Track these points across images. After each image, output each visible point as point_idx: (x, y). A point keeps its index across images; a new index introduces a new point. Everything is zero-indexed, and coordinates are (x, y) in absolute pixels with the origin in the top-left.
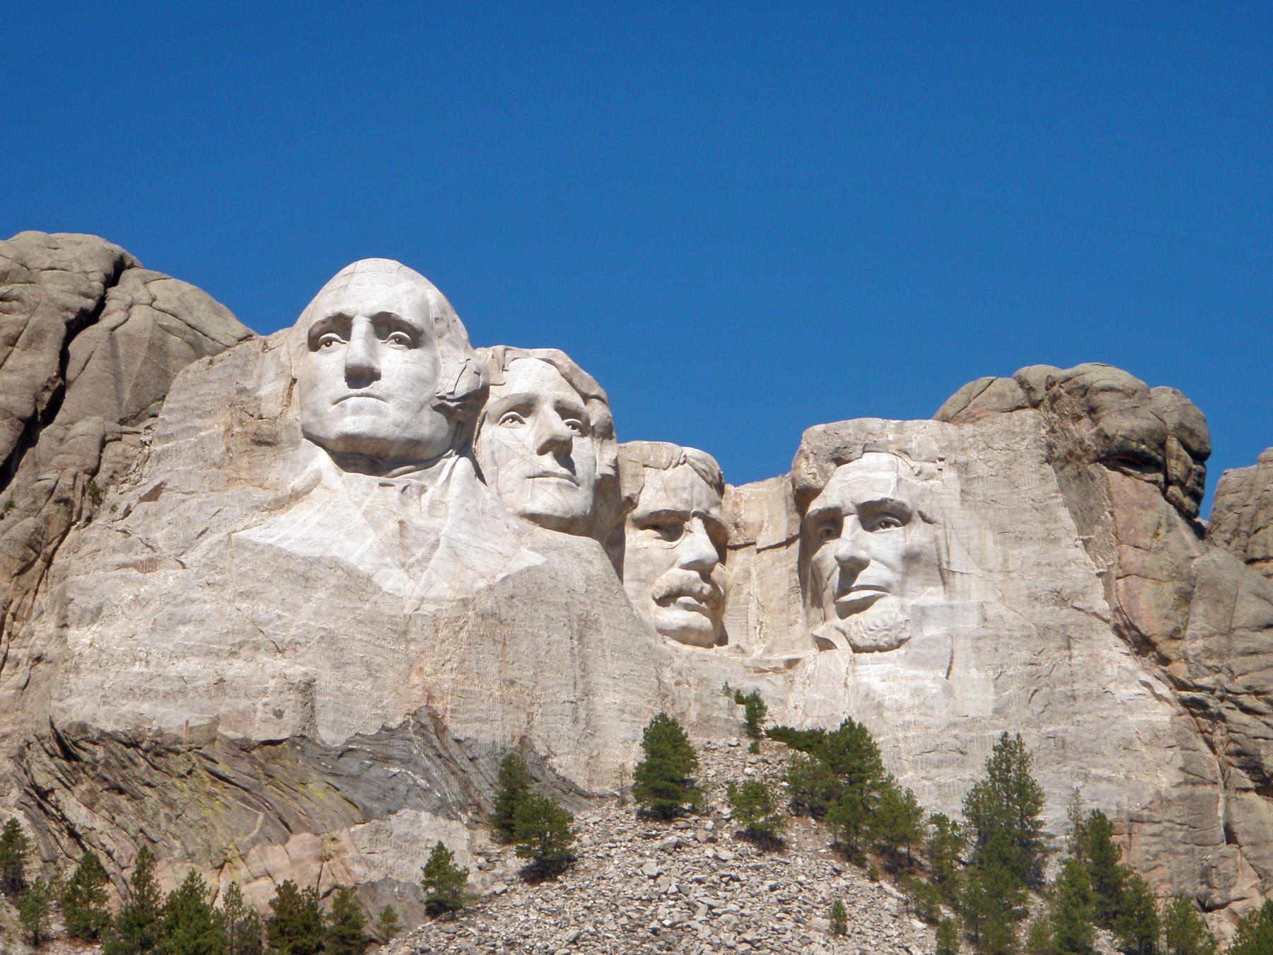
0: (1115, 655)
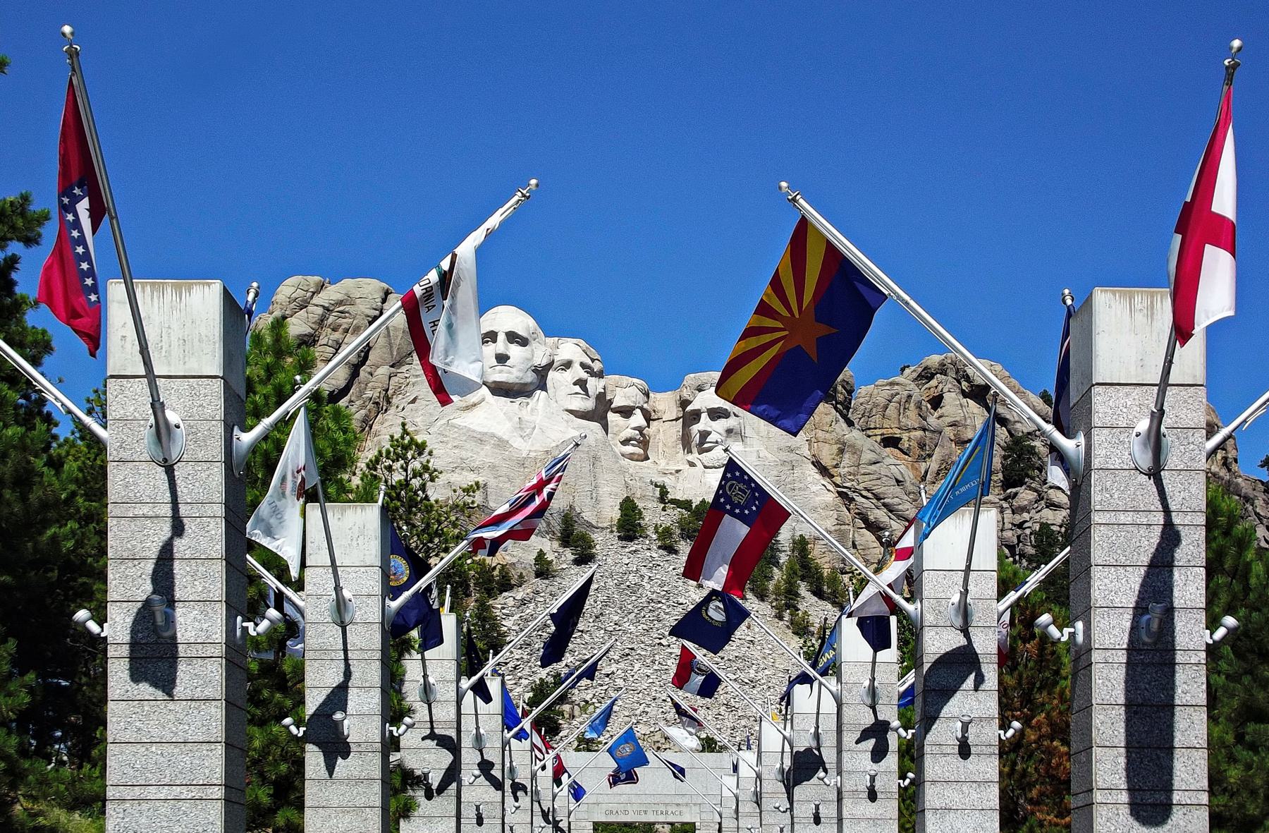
0: (812, 473)
